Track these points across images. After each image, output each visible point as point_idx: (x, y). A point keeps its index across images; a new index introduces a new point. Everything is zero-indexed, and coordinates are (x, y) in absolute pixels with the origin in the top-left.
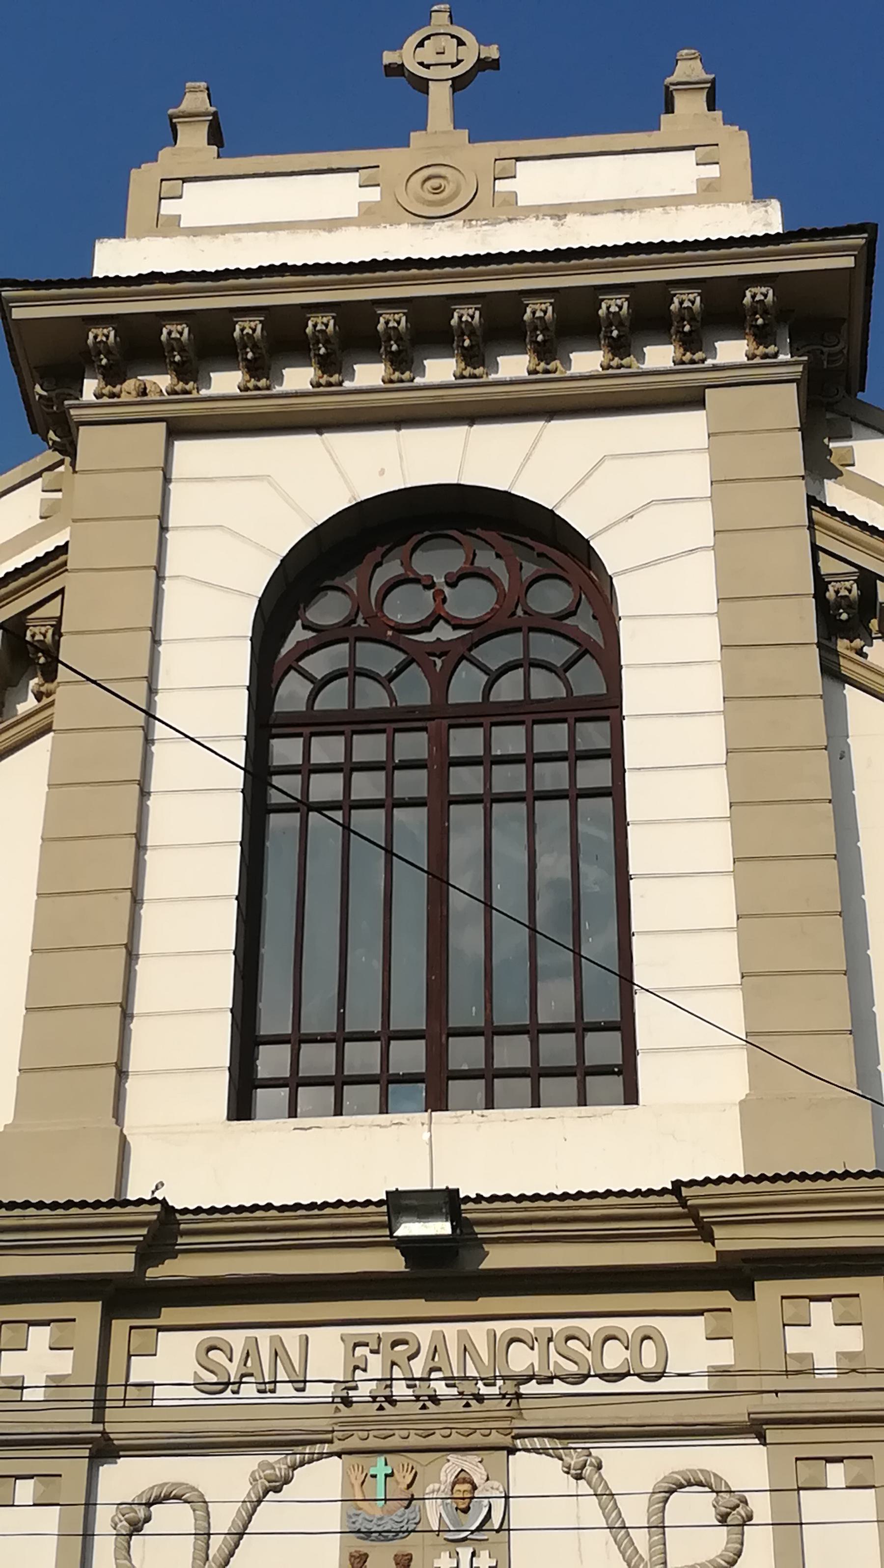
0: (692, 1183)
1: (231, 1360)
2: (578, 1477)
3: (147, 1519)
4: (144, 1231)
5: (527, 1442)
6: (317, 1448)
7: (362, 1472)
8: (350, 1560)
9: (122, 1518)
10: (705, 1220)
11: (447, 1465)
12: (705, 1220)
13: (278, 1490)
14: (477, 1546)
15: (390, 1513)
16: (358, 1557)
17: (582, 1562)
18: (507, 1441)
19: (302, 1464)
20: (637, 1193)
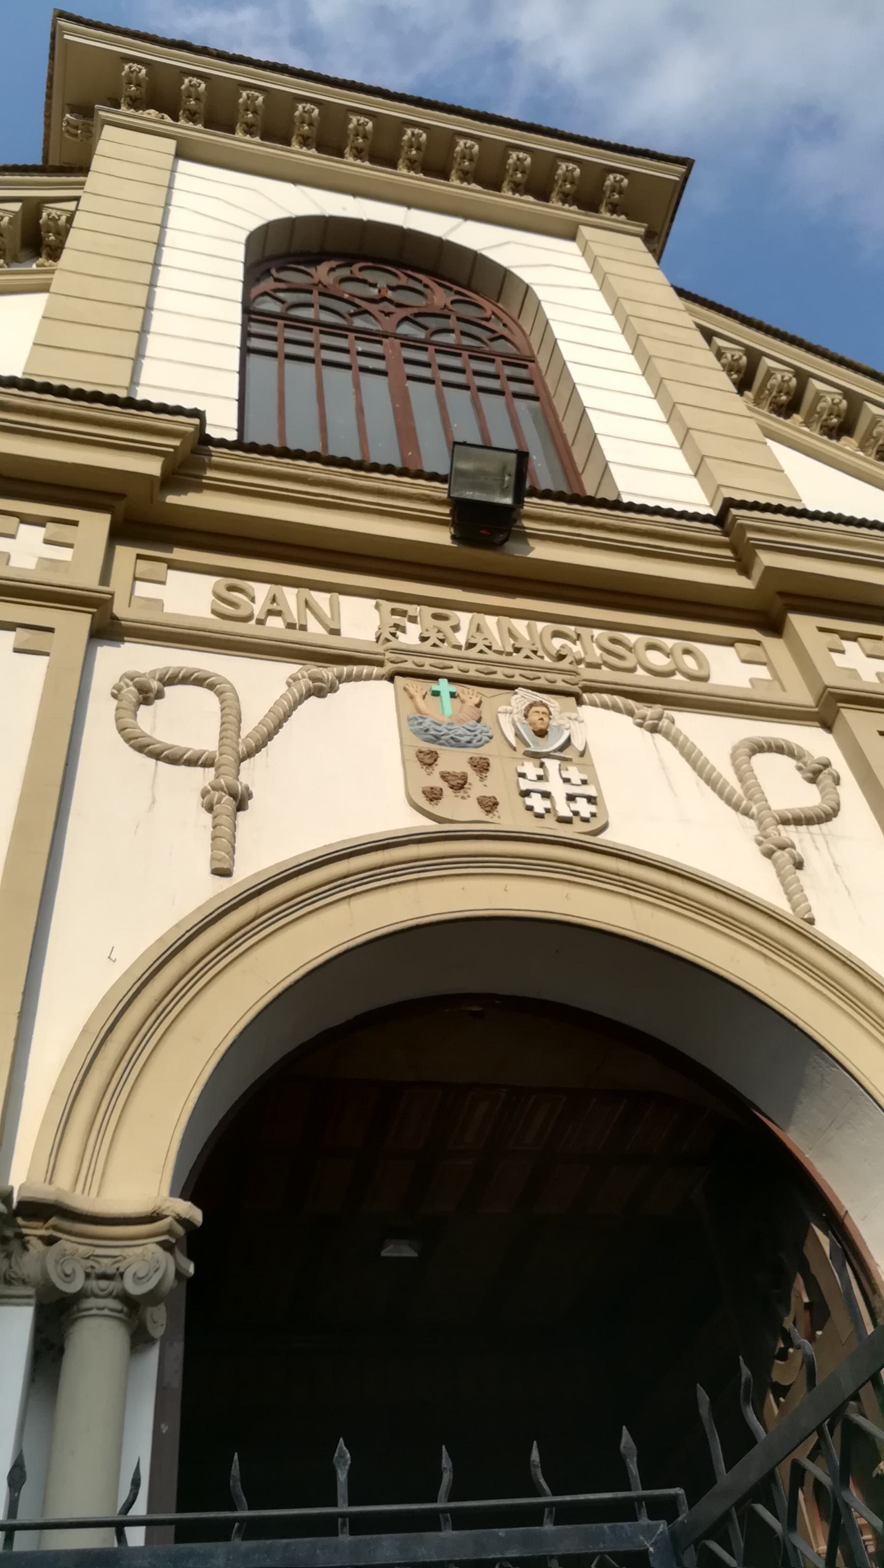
0: (743, 505)
1: (253, 600)
2: (654, 729)
3: (160, 695)
4: (177, 443)
5: (595, 697)
6: (366, 669)
7: (422, 689)
8: (417, 756)
9: (130, 683)
10: (751, 542)
11: (515, 696)
12: (751, 542)
13: (320, 693)
14: (564, 764)
16: (428, 754)
17: (676, 795)
18: (576, 689)
19: (349, 678)
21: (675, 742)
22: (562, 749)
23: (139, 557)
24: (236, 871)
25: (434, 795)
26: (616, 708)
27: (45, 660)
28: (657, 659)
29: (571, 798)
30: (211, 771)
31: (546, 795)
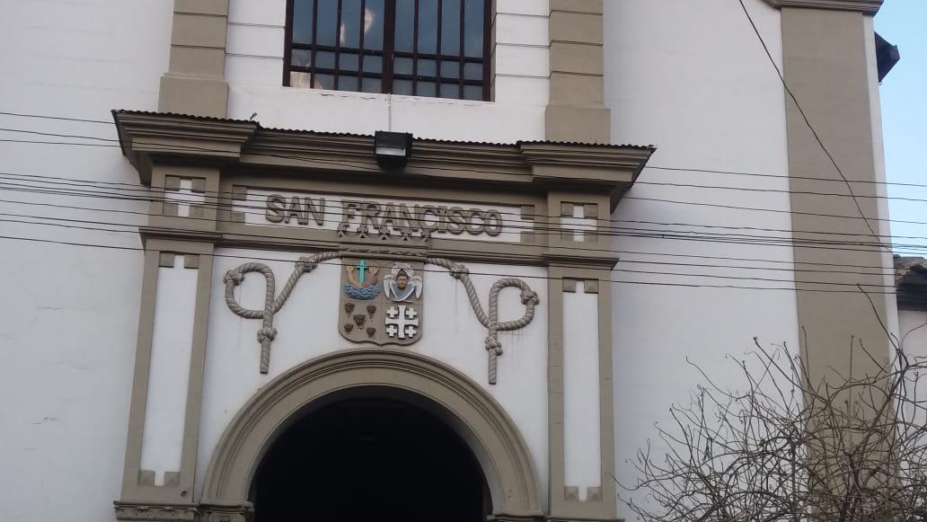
0: (528, 143)
2: (457, 278)
3: (242, 280)
4: (246, 138)
5: (434, 259)
6: (330, 254)
13: (308, 271)
15: (366, 286)
20: (498, 145)
21: (465, 285)
22: (409, 298)
23: (234, 186)
24: (270, 370)
25: (348, 329)
27: (197, 270)
29: (407, 327)
30: (262, 320)
31: (396, 326)
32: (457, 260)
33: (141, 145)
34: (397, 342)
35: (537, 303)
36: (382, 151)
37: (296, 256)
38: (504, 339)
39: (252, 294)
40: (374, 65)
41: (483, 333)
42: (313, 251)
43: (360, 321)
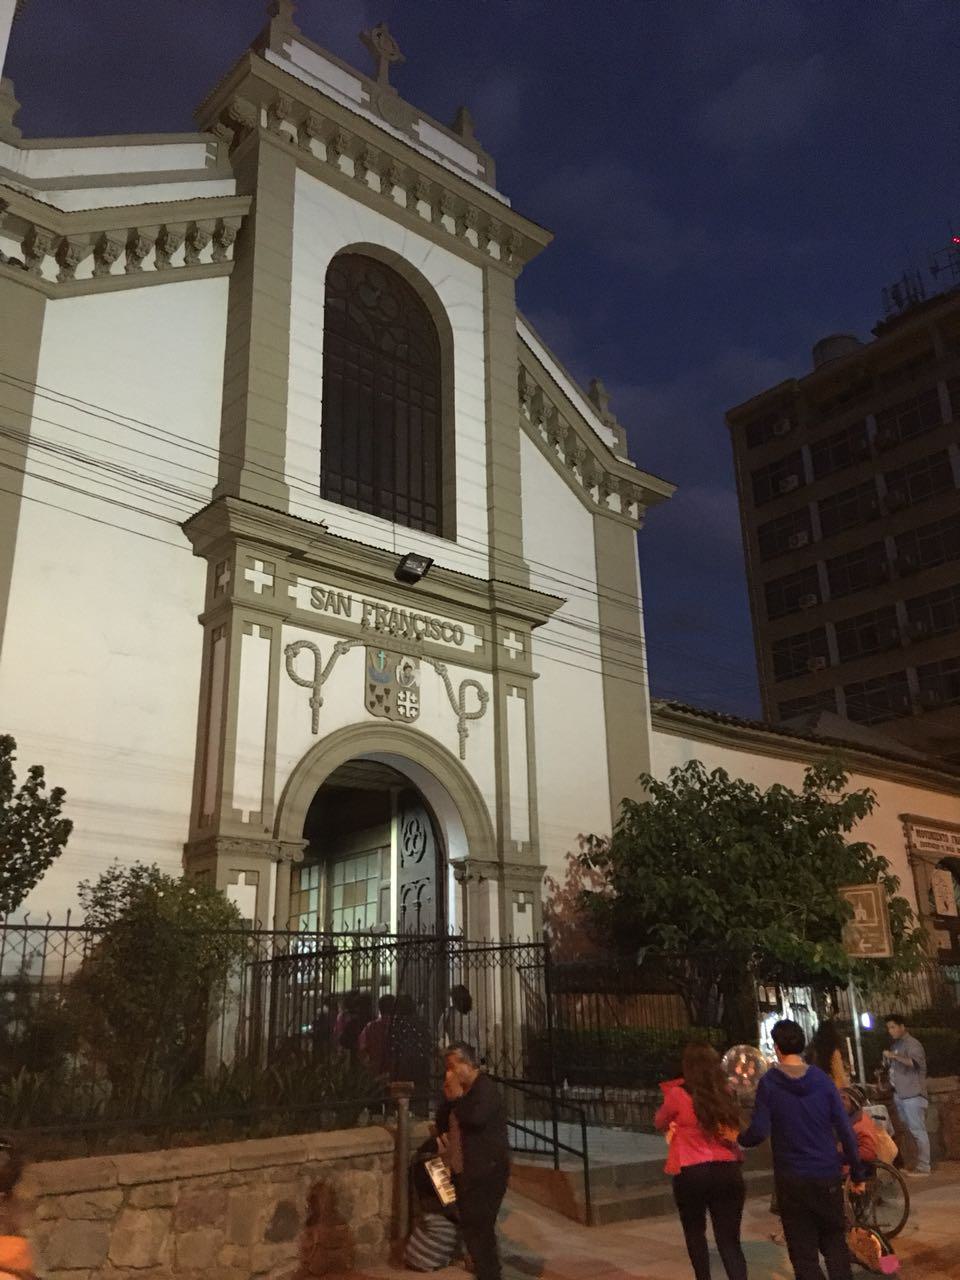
5: (423, 657)
13: (343, 653)
21: (445, 681)
25: (372, 704)
26: (431, 663)
28: (448, 633)
31: (404, 707)
32: (441, 659)
33: (237, 526)
34: (403, 718)
35: (488, 700)
36: (410, 564)
37: (334, 640)
38: (468, 724)
39: (304, 665)
40: (366, 490)
41: (456, 719)
42: (348, 636)
43: (379, 698)
